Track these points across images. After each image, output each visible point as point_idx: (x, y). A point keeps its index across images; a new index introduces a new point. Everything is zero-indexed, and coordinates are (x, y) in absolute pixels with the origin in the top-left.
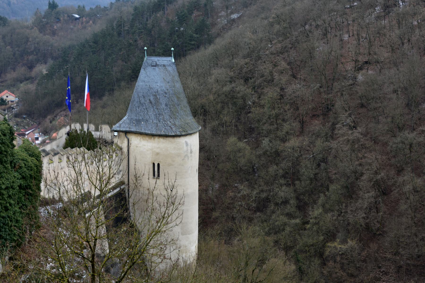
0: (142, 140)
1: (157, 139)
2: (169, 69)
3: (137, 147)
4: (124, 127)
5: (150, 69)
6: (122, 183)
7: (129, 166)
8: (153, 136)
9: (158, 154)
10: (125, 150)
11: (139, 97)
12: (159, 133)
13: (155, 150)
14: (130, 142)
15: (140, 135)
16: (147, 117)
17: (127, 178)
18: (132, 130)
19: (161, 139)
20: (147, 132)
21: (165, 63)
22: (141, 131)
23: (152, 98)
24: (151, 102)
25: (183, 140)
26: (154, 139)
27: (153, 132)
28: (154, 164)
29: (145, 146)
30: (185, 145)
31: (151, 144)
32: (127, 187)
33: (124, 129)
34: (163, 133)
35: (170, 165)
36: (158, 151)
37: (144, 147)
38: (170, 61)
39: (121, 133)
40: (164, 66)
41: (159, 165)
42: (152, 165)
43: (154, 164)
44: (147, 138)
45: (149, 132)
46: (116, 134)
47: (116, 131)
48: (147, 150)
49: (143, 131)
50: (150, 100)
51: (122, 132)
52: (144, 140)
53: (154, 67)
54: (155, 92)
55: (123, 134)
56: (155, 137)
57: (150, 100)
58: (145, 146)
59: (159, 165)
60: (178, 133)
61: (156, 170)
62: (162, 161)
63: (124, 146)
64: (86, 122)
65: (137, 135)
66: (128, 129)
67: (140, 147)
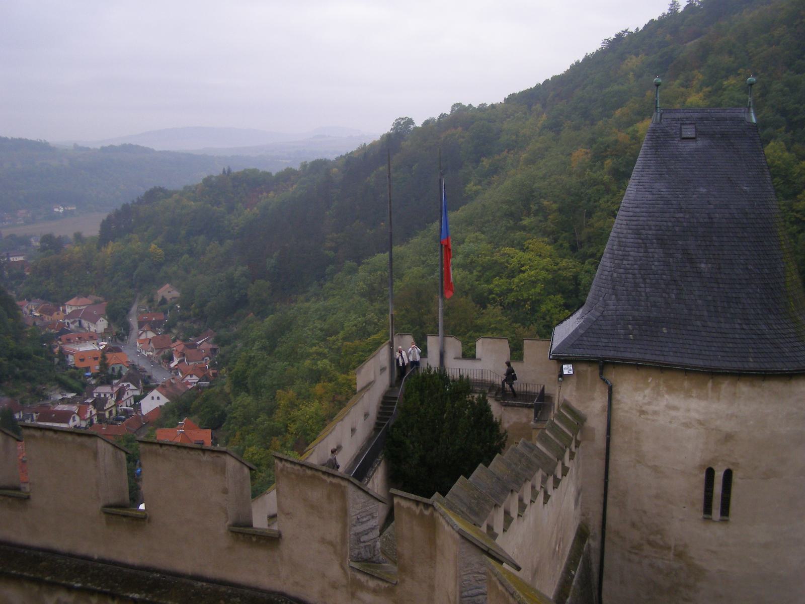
0: (663, 389)
1: (725, 386)
3: (642, 412)
8: (714, 374)
9: (728, 437)
13: (718, 423)
14: (617, 396)
19: (743, 388)
20: (687, 361)
28: (710, 473)
29: (675, 408)
33: (599, 353)
34: (751, 365)
36: (728, 426)
37: (673, 413)
39: (583, 368)
41: (728, 475)
42: (703, 476)
43: (710, 473)
44: (686, 384)
45: (700, 363)
46: (567, 369)
48: (687, 425)
49: (670, 359)
52: (671, 390)
55: (590, 371)
58: (675, 408)
59: (728, 475)
61: (717, 492)
63: (593, 407)
64: (435, 333)
66: (611, 354)
67: (655, 413)
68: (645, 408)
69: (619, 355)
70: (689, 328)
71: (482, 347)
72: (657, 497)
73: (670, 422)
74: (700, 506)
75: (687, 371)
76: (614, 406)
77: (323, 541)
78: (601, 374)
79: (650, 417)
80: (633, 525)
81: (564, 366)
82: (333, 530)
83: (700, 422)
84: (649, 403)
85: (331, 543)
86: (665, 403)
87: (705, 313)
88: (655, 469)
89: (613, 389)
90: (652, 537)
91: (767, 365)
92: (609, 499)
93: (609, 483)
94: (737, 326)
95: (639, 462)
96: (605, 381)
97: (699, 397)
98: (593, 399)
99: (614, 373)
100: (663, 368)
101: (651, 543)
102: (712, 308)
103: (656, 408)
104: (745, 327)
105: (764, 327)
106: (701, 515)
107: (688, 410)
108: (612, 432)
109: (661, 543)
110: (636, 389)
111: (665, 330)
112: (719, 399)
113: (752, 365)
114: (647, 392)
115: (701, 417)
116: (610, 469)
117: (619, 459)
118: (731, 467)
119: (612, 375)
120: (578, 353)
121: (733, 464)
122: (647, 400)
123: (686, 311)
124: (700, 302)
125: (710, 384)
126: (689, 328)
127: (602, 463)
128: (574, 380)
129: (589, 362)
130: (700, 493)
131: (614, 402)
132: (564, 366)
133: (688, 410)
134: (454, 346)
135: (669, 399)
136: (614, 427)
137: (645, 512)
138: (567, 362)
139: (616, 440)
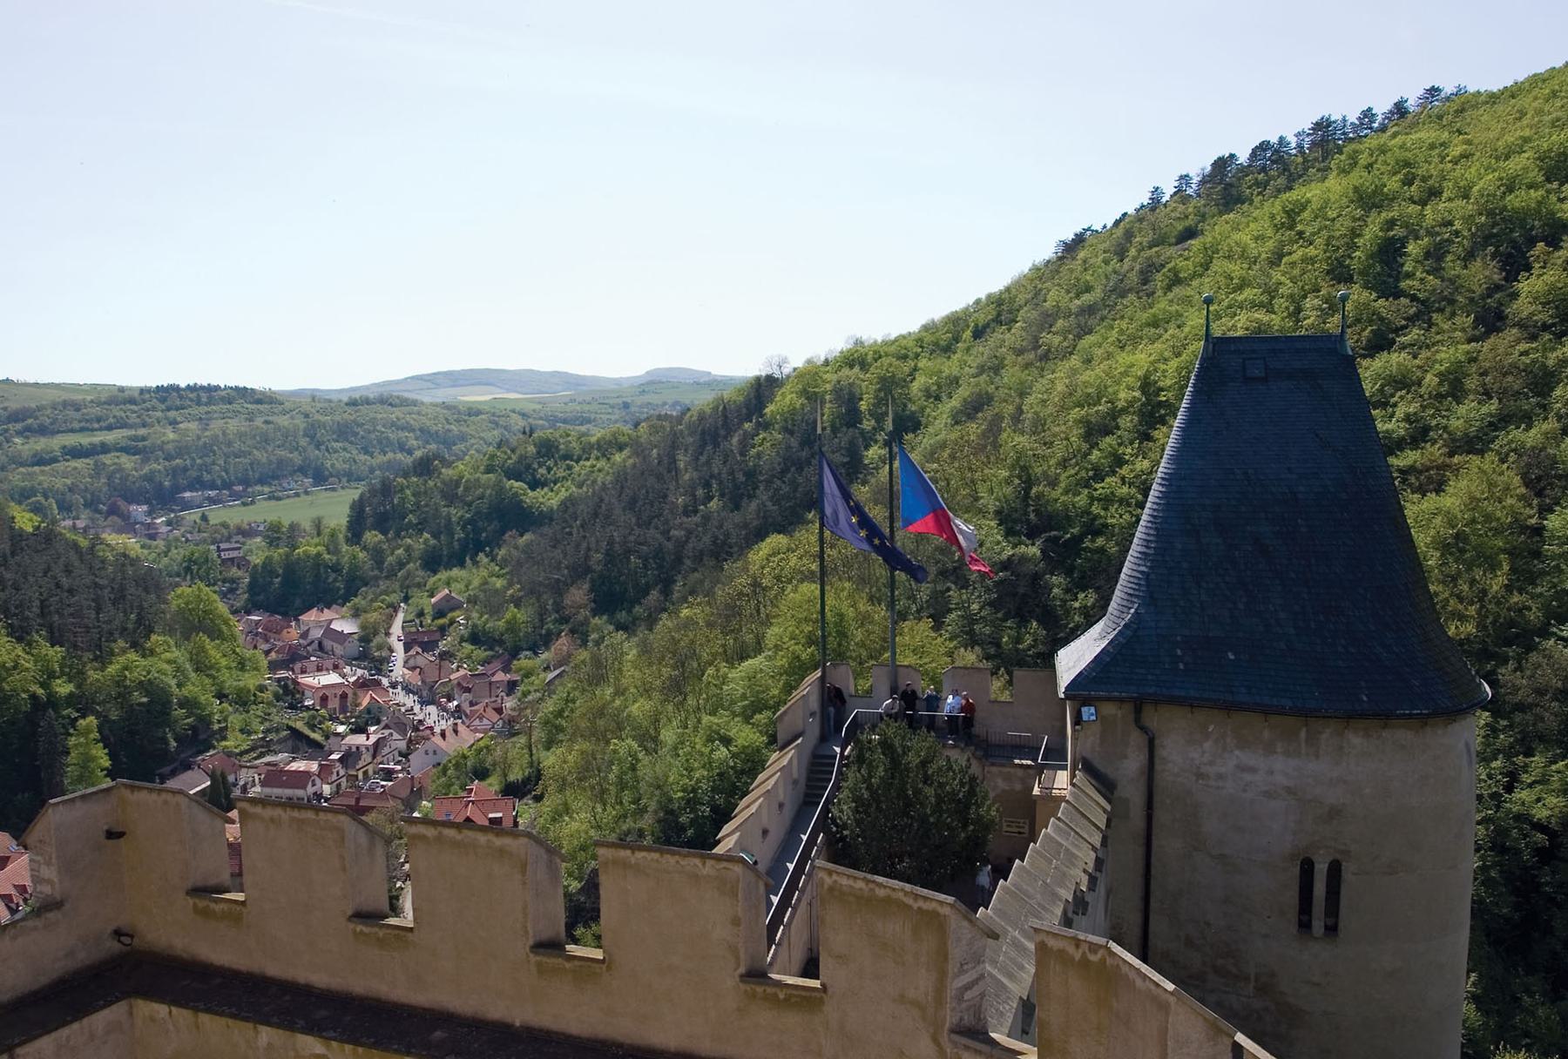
9: (1335, 813)
14: (1161, 753)
28: (1307, 868)
29: (1252, 770)
37: (1248, 777)
41: (1335, 870)
42: (1297, 870)
43: (1307, 868)
48: (1268, 795)
58: (1252, 770)
59: (1335, 870)
67: (1220, 777)
68: (1204, 770)
73: (1245, 791)
74: (1293, 915)
76: (1158, 767)
77: (902, 999)
79: (1212, 783)
81: (1084, 709)
82: (922, 984)
83: (1289, 790)
84: (1211, 763)
85: (915, 1003)
87: (1292, 631)
89: (1157, 742)
90: (1220, 962)
92: (1154, 904)
93: (1153, 882)
94: (1340, 649)
96: (1143, 729)
98: (1126, 757)
103: (1223, 770)
106: (1294, 929)
108: (1156, 805)
109: (1234, 970)
112: (1317, 756)
114: (1207, 745)
117: (1168, 845)
118: (1338, 857)
124: (1282, 615)
125: (1303, 734)
127: (1141, 851)
130: (1292, 897)
131: (1157, 761)
132: (1084, 709)
138: (1087, 702)
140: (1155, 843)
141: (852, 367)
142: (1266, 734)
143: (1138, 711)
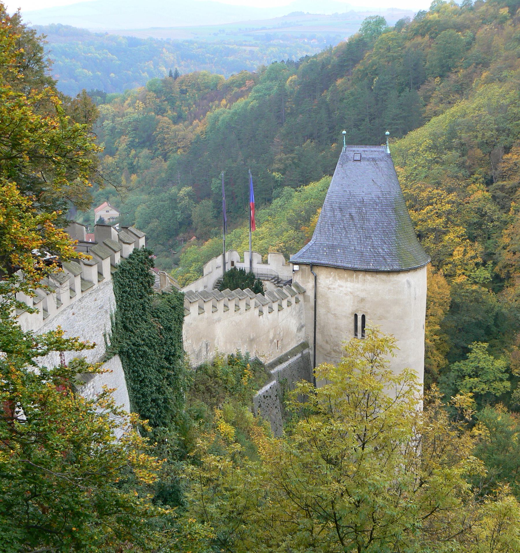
0: (337, 277)
1: (361, 276)
2: (382, 164)
3: (329, 288)
4: (309, 258)
5: (351, 164)
6: (304, 345)
7: (315, 319)
8: (356, 270)
9: (362, 300)
10: (310, 293)
11: (333, 210)
12: (366, 267)
13: (358, 293)
14: (319, 281)
15: (334, 270)
16: (346, 242)
17: (313, 339)
18: (322, 262)
19: (369, 277)
20: (345, 265)
21: (375, 155)
22: (336, 264)
23: (353, 211)
24: (352, 217)
25: (403, 278)
26: (357, 276)
27: (356, 266)
29: (342, 286)
30: (406, 286)
31: (352, 284)
32: (312, 352)
33: (310, 261)
34: (371, 267)
35: (380, 318)
36: (363, 295)
37: (341, 289)
38: (383, 152)
39: (304, 267)
40: (374, 160)
41: (363, 317)
42: (353, 318)
43: (356, 316)
45: (350, 266)
46: (296, 267)
47: (296, 264)
48: (346, 294)
49: (339, 264)
50: (350, 214)
51: (306, 264)
52: (340, 278)
53: (359, 163)
54: (360, 202)
55: (307, 268)
56: (358, 273)
57: (350, 214)
58: (342, 286)
59: (363, 317)
60: (396, 267)
62: (368, 311)
63: (309, 286)
65: (329, 270)
66: (315, 261)
67: (334, 289)
68: (330, 287)
69: (319, 261)
70: (349, 250)
71: (270, 258)
72: (336, 328)
74: (353, 332)
75: (345, 269)
76: (318, 286)
78: (311, 270)
79: (332, 291)
80: (327, 342)
83: (351, 293)
84: (332, 284)
86: (338, 284)
88: (335, 315)
89: (317, 278)
90: (335, 348)
91: (378, 267)
93: (317, 322)
94: (368, 250)
95: (329, 312)
97: (350, 281)
99: (355, 276)
100: (336, 268)
101: (335, 351)
102: (359, 241)
104: (372, 250)
105: (380, 250)
107: (347, 287)
108: (317, 298)
109: (338, 350)
110: (327, 278)
111: (339, 251)
113: (371, 267)
114: (331, 279)
115: (351, 291)
116: (317, 316)
117: (321, 311)
118: (364, 314)
119: (316, 271)
120: (301, 260)
121: (365, 312)
122: (331, 282)
123: (348, 242)
124: (354, 238)
125: (355, 276)
126: (349, 250)
128: (300, 273)
129: (306, 264)
130: (352, 326)
131: (317, 284)
132: (295, 266)
133: (347, 287)
134: (257, 257)
135: (339, 282)
136: (318, 296)
137: (332, 336)
139: (319, 301)
140: (317, 308)
141: (423, 35)
142: (346, 275)
143: (311, 268)
